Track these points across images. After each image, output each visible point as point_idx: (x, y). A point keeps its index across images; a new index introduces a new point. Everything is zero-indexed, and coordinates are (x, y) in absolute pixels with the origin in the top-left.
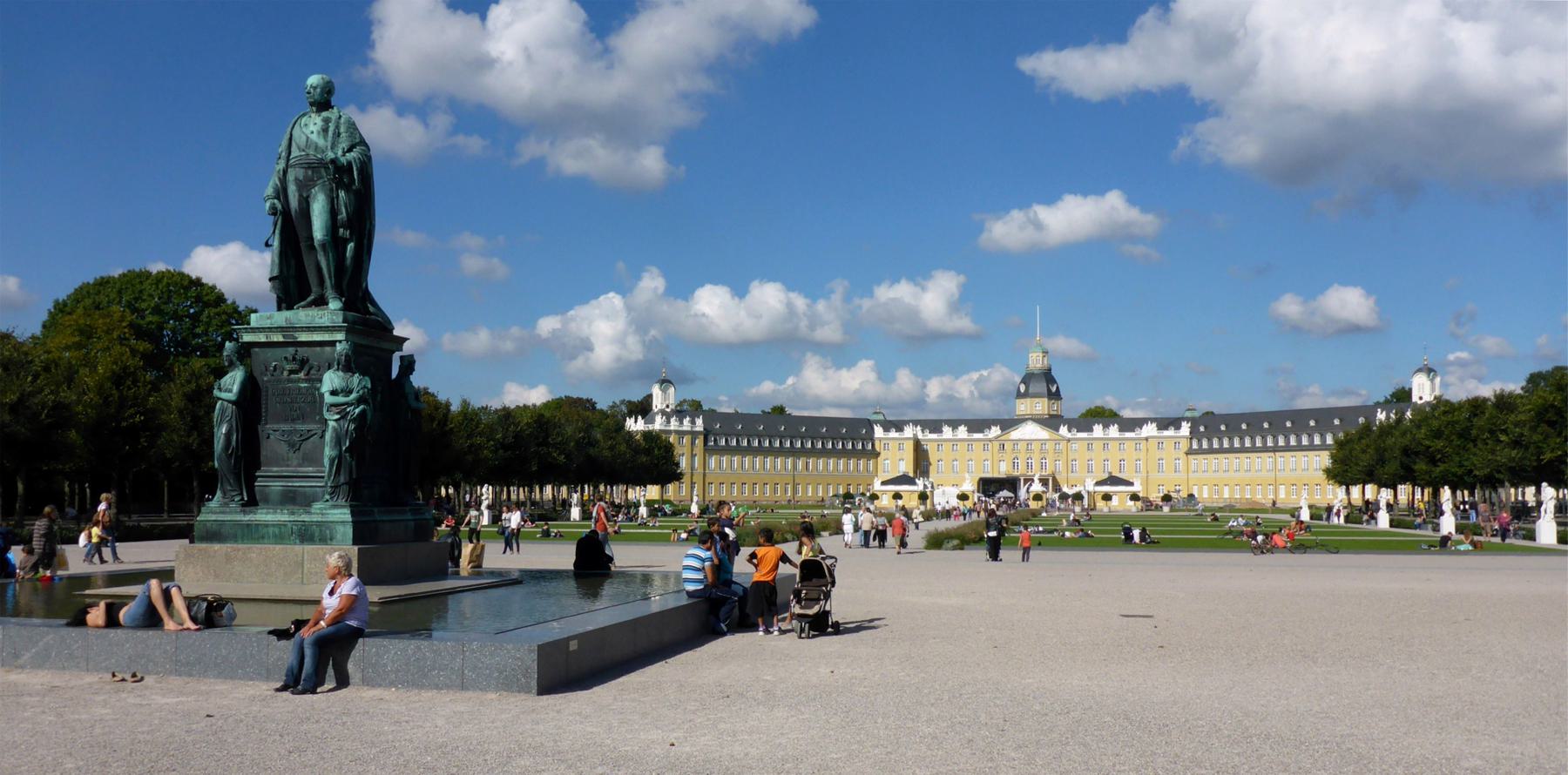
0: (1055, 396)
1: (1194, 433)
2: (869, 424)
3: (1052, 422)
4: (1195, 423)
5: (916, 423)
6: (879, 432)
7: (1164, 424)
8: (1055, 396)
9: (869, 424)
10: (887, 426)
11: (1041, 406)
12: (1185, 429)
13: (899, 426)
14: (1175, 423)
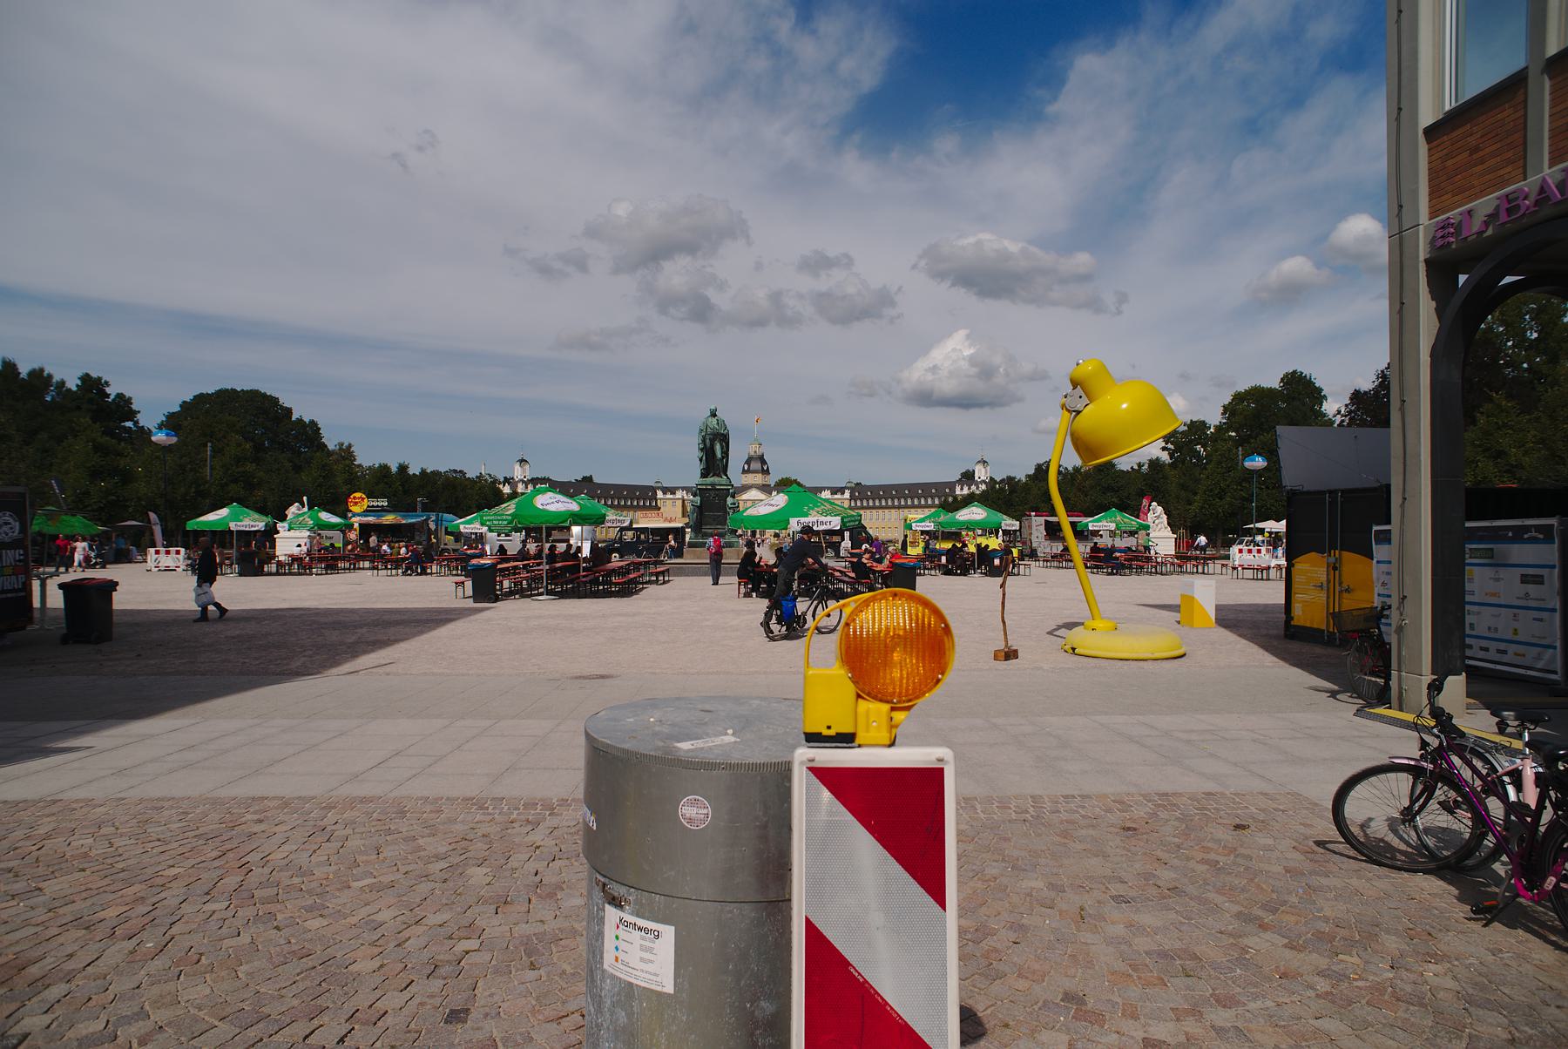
0: (766, 472)
1: (852, 497)
2: (654, 490)
3: (766, 489)
4: (852, 490)
5: (683, 489)
6: (660, 494)
7: (835, 491)
8: (766, 472)
9: (654, 490)
10: (665, 490)
11: (758, 479)
12: (847, 494)
13: (673, 491)
14: (841, 490)
